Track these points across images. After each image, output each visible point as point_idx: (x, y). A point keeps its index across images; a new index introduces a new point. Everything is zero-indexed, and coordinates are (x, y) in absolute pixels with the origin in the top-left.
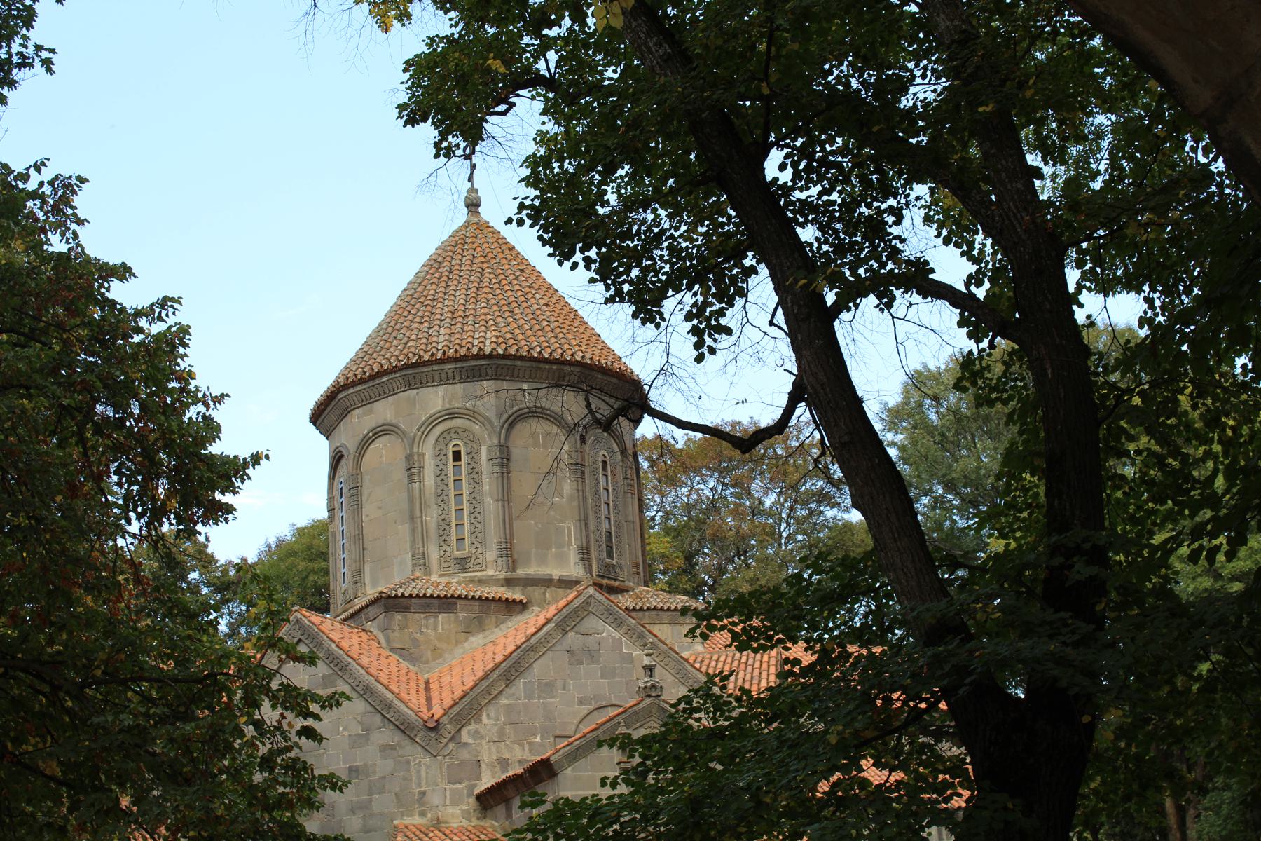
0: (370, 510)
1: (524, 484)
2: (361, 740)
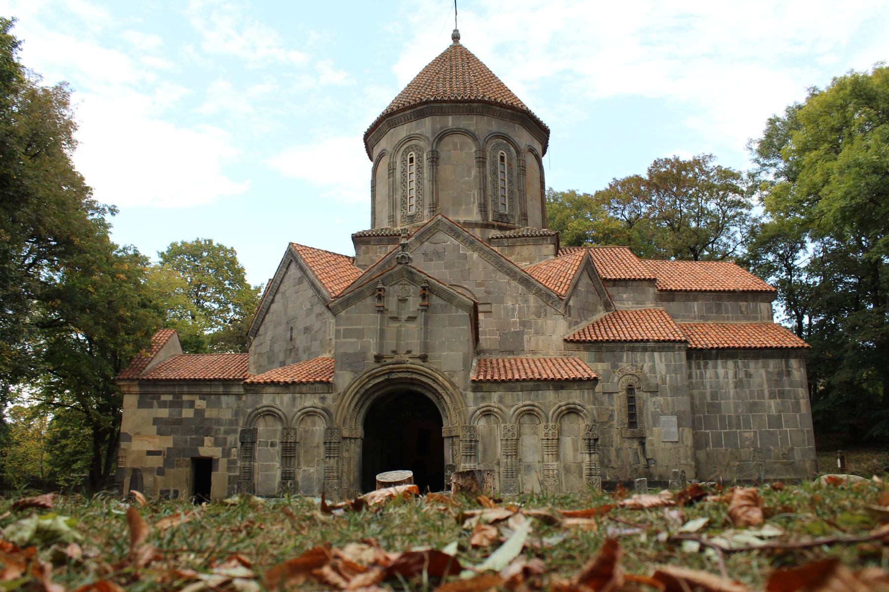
0: (378, 198)
1: (446, 171)
2: (310, 310)
